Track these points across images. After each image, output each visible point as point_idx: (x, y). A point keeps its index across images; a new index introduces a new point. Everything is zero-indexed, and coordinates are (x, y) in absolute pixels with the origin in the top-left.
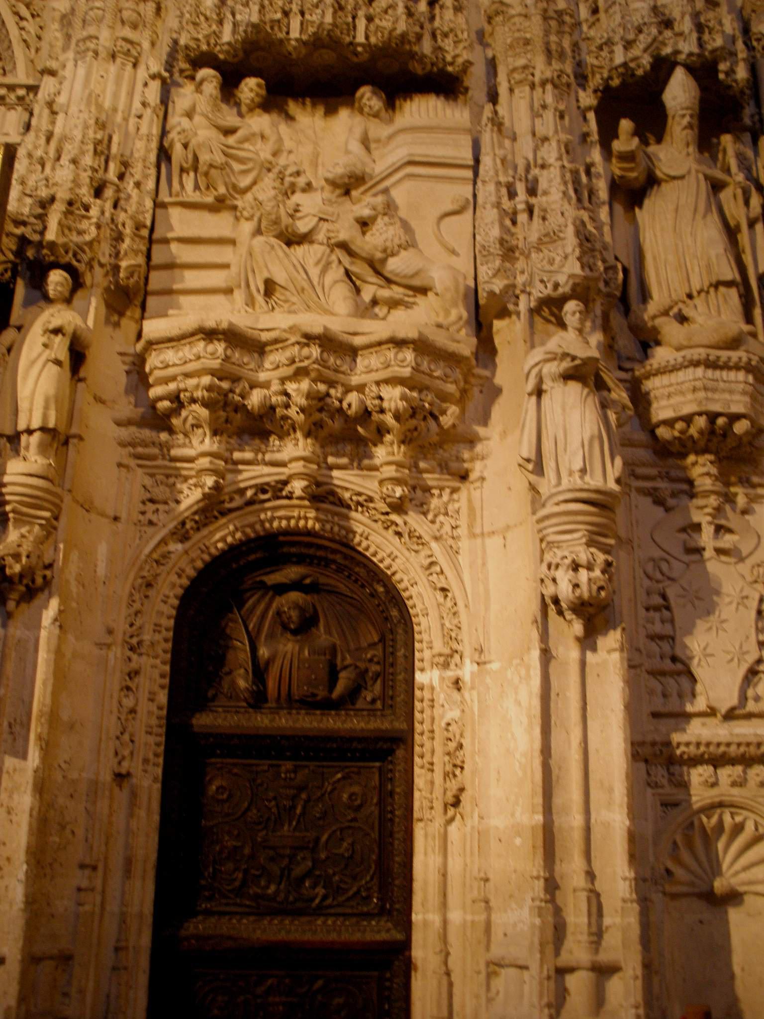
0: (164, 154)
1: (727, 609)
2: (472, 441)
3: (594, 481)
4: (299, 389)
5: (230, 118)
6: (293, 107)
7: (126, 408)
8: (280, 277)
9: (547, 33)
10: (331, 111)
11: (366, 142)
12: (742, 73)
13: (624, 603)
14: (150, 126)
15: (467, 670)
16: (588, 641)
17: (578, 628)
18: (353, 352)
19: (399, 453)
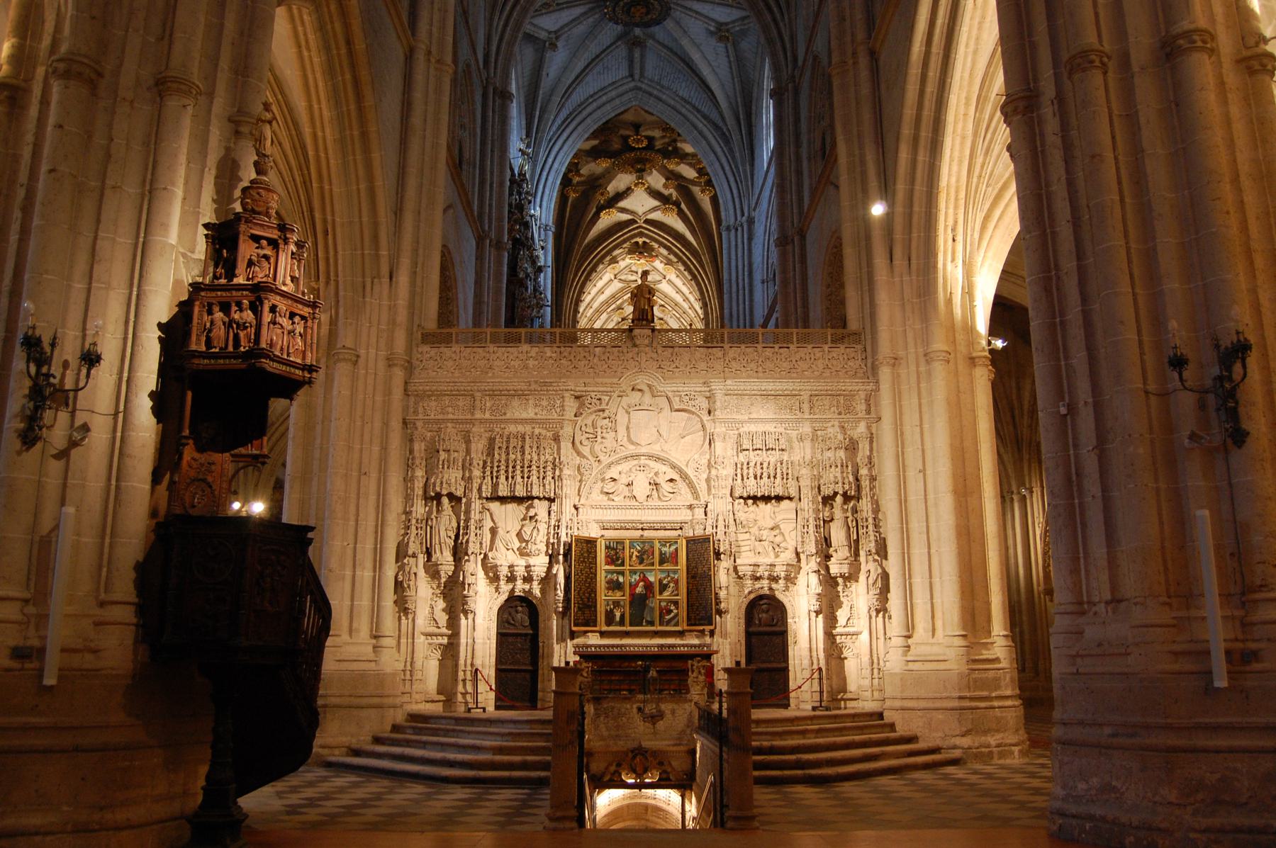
0: (735, 520)
1: (844, 606)
4: (766, 574)
5: (747, 509)
6: (758, 502)
7: (734, 575)
10: (766, 504)
12: (853, 493)
13: (823, 611)
16: (817, 617)
17: (815, 614)
19: (784, 582)
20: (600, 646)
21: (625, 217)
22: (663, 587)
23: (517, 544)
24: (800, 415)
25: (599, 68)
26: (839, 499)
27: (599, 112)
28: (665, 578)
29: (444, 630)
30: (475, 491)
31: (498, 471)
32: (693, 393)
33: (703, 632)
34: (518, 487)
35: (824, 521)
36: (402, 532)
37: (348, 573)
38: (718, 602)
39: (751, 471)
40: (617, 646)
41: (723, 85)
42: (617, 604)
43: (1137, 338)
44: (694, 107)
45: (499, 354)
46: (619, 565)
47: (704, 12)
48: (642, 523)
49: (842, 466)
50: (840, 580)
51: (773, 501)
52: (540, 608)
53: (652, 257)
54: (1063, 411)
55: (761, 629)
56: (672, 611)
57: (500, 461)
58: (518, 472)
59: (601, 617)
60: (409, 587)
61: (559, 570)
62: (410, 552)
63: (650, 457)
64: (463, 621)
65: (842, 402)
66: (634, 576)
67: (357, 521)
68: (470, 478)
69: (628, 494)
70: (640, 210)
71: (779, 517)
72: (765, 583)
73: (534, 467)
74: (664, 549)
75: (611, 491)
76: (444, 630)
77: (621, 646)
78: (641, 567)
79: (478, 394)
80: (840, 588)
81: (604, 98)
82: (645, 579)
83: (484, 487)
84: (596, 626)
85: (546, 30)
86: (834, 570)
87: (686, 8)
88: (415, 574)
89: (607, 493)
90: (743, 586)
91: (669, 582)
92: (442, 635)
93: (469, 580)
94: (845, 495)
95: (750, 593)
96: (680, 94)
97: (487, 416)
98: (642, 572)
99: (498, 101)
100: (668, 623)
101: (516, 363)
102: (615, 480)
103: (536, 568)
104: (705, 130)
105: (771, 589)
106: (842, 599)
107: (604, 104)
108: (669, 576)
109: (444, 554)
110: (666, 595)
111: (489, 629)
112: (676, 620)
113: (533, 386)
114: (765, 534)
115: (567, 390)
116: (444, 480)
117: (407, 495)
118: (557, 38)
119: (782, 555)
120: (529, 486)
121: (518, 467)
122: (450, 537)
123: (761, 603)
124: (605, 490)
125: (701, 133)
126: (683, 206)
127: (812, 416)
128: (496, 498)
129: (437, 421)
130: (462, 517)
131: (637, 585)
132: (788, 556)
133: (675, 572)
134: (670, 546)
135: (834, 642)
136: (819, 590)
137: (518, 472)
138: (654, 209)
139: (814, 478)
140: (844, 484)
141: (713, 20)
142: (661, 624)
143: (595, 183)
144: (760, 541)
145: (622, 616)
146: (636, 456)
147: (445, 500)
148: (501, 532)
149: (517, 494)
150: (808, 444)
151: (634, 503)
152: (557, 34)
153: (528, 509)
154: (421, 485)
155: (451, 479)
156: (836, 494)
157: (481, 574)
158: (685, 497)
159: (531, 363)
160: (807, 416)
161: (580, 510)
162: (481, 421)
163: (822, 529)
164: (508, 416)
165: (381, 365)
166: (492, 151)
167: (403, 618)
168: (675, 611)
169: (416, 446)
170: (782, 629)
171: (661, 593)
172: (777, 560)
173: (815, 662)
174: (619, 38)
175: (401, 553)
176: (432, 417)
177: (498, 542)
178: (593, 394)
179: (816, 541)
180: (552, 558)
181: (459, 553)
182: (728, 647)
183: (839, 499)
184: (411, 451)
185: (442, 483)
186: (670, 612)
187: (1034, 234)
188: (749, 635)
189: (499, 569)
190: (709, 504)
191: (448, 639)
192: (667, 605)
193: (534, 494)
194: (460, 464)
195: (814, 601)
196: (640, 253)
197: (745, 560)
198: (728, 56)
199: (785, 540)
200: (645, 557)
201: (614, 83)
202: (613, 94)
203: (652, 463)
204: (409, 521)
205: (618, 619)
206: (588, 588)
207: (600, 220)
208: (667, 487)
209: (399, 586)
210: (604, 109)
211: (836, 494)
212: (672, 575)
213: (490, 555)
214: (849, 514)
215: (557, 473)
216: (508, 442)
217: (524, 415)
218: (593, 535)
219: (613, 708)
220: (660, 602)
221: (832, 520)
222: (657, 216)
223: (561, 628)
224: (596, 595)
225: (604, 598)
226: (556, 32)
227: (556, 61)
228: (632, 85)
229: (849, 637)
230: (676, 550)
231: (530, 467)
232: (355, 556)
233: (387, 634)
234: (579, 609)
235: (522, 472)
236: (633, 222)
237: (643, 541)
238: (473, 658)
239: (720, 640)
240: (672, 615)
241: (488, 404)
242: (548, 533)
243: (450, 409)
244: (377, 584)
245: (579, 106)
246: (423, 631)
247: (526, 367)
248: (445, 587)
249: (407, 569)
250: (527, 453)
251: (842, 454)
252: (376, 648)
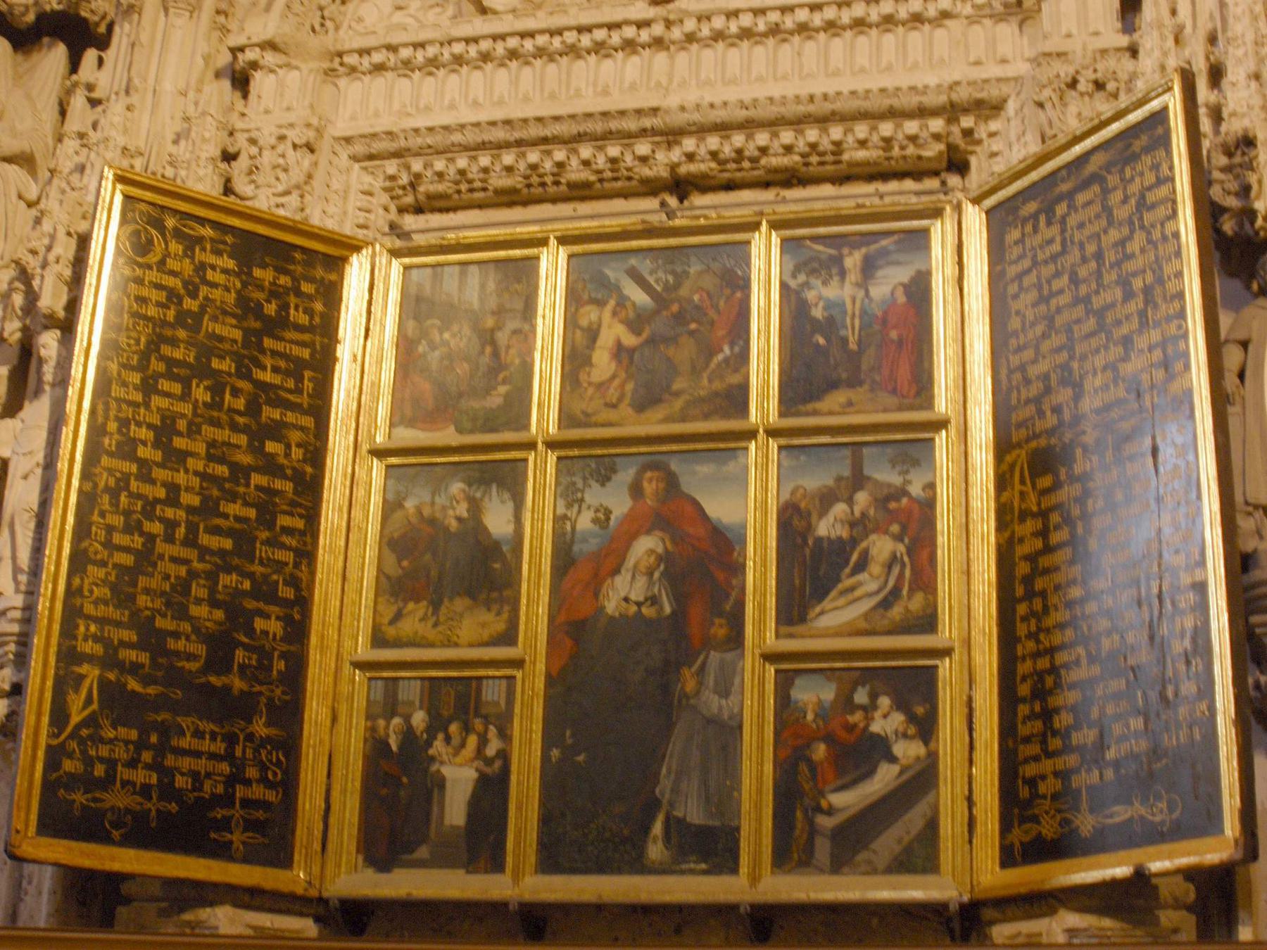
28: (827, 499)
56: (879, 749)
66: (595, 495)
84: (281, 856)
91: (861, 526)
108: (858, 480)
112: (914, 819)
134: (869, 268)
168: (911, 750)
192: (846, 703)
200: (684, 352)
205: (455, 810)
212: (887, 476)
220: (785, 682)
224: (298, 630)
225: (363, 650)
240: (884, 778)
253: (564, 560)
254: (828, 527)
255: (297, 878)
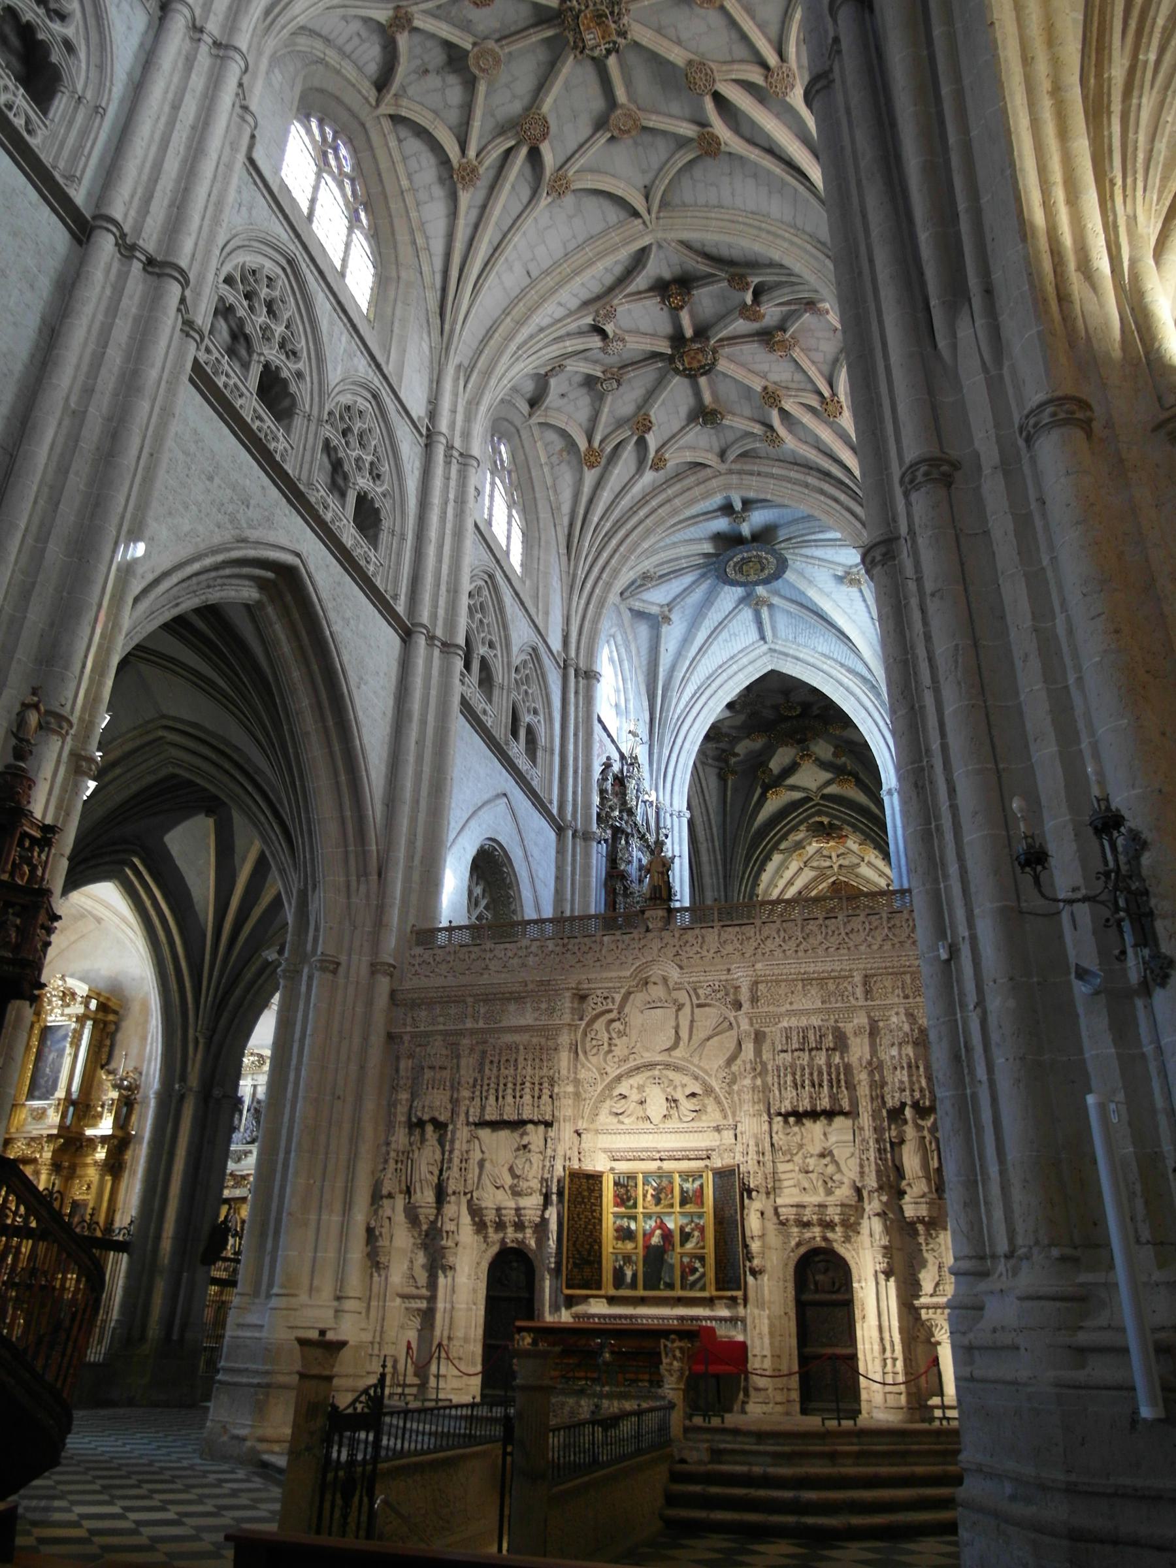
0: (772, 1145)
2: (859, 1224)
3: (883, 1243)
4: (815, 1217)
5: (788, 1130)
6: (805, 1121)
7: (775, 1220)
8: (806, 1186)
9: (871, 1090)
10: (815, 1122)
11: (825, 1134)
12: (927, 1103)
14: (768, 1139)
15: (863, 1284)
16: (887, 1280)
18: (826, 1206)
20: (604, 1316)
21: (798, 795)
22: (685, 1237)
23: (508, 1180)
24: (853, 1002)
25: (725, 635)
26: (908, 1113)
27: (731, 683)
29: (424, 1292)
30: (462, 1117)
31: (488, 1091)
32: (717, 983)
33: (734, 1299)
34: (507, 1109)
35: (892, 1143)
36: (381, 1167)
37: (313, 1217)
38: (749, 1257)
39: (789, 1078)
40: (626, 1317)
41: (863, 633)
42: (627, 1259)
43: (1004, 833)
44: (835, 660)
45: (496, 952)
46: (630, 1208)
47: (828, 557)
48: (659, 1152)
49: (910, 1066)
50: (920, 1227)
51: (822, 1118)
52: (536, 1263)
53: (841, 837)
54: (944, 955)
55: (817, 1297)
56: (696, 1270)
57: (489, 1078)
58: (509, 1091)
59: (607, 1275)
60: (381, 1234)
61: (552, 1214)
62: (385, 1192)
63: (667, 1066)
64: (441, 1280)
65: (909, 981)
66: (649, 1222)
67: (327, 1153)
68: (457, 1100)
69: (641, 1114)
70: (813, 786)
71: (833, 1139)
72: (817, 1230)
73: (528, 1084)
74: (686, 1186)
75: (620, 1111)
76: (424, 1292)
77: (631, 1317)
78: (658, 1209)
79: (470, 1000)
80: (921, 1240)
81: (735, 667)
82: (662, 1226)
83: (472, 1110)
84: (599, 1288)
85: (658, 605)
86: (909, 1212)
87: (807, 557)
88: (390, 1218)
89: (617, 1114)
90: (788, 1236)
91: (693, 1230)
92: (420, 1297)
93: (449, 1226)
94: (916, 1105)
95: (798, 1245)
96: (820, 650)
97: (481, 1024)
98: (659, 1216)
99: (582, 682)
100: (693, 1285)
101: (516, 961)
102: (625, 1097)
103: (527, 1212)
104: (851, 684)
105: (825, 1239)
106: (926, 1255)
107: (736, 673)
109: (426, 1193)
110: (689, 1246)
111: (475, 1291)
112: (702, 1282)
113: (530, 987)
114: (812, 1162)
115: (568, 989)
116: (427, 1103)
117: (390, 1121)
118: (670, 611)
119: (838, 1192)
120: (519, 1108)
121: (510, 1085)
122: (432, 1173)
123: (817, 1259)
124: (615, 1110)
125: (847, 689)
126: (862, 776)
127: (869, 1003)
128: (483, 1124)
129: (427, 1034)
130: (447, 1148)
131: (652, 1234)
132: (844, 1193)
133: (700, 1215)
135: (918, 1318)
136: (885, 1241)
137: (509, 1091)
138: (828, 783)
139: (873, 1084)
140: (913, 1091)
141: (839, 564)
142: (683, 1288)
143: (759, 761)
144: (807, 1172)
145: (635, 1276)
146: (650, 1066)
147: (429, 1128)
148: (487, 1165)
149: (505, 1117)
150: (866, 1041)
151: (648, 1125)
152: (670, 606)
153: (522, 1135)
154: (405, 1110)
155: (436, 1102)
156: (903, 1105)
157: (466, 1219)
158: (713, 1116)
159: (531, 960)
160: (861, 1002)
161: (583, 1136)
162: (473, 1032)
163: (889, 1155)
164: (504, 1024)
165: (364, 970)
166: (576, 735)
167: (375, 1274)
168: (701, 1270)
169: (403, 1064)
170: (847, 1297)
171: (682, 1245)
172: (830, 1198)
173: (888, 1347)
174: (742, 600)
175: (377, 1197)
176: (422, 1029)
177: (484, 1177)
178: (599, 992)
179: (878, 1172)
180: (547, 1197)
181: (441, 1195)
182: (766, 1321)
183: (908, 1113)
184: (397, 1070)
185: (424, 1107)
186: (694, 1270)
187: (899, 713)
188: (802, 1306)
189: (485, 1212)
190: (739, 1125)
191: (428, 1303)
193: (525, 1117)
194: (448, 1084)
195: (880, 1258)
196: (828, 834)
197: (788, 1197)
198: (865, 600)
199: (839, 1170)
201: (742, 651)
202: (745, 661)
203: (671, 1074)
204: (388, 1153)
205: (629, 1279)
206: (589, 1237)
207: (769, 802)
208: (686, 1105)
209: (371, 1234)
210: (736, 679)
211: (903, 1105)
212: (697, 1221)
213: (475, 1194)
214: (926, 1133)
215: (556, 1090)
216: (500, 1054)
217: (523, 1022)
218: (599, 1168)
219: (563, 1404)
221: (902, 1142)
222: (832, 789)
223: (556, 1291)
224: (600, 1247)
225: (611, 1250)
226: (668, 605)
227: (672, 636)
228: (765, 648)
229: (939, 1311)
230: (701, 1186)
231: (523, 1083)
232: (322, 1197)
233: (351, 1295)
234: (575, 1264)
235: (514, 1090)
236: (808, 799)
237: (661, 1175)
238: (450, 1329)
239: (756, 1311)
240: (697, 1275)
241: (482, 1011)
242: (544, 1166)
243: (441, 1019)
244: (344, 1234)
245: (708, 678)
246: (400, 1291)
247: (524, 965)
248: (427, 1235)
249: (380, 1212)
250: (520, 1067)
251: (909, 1050)
252: (337, 1311)
253: (645, 1235)
254: (687, 1230)
255: (602, 1292)
